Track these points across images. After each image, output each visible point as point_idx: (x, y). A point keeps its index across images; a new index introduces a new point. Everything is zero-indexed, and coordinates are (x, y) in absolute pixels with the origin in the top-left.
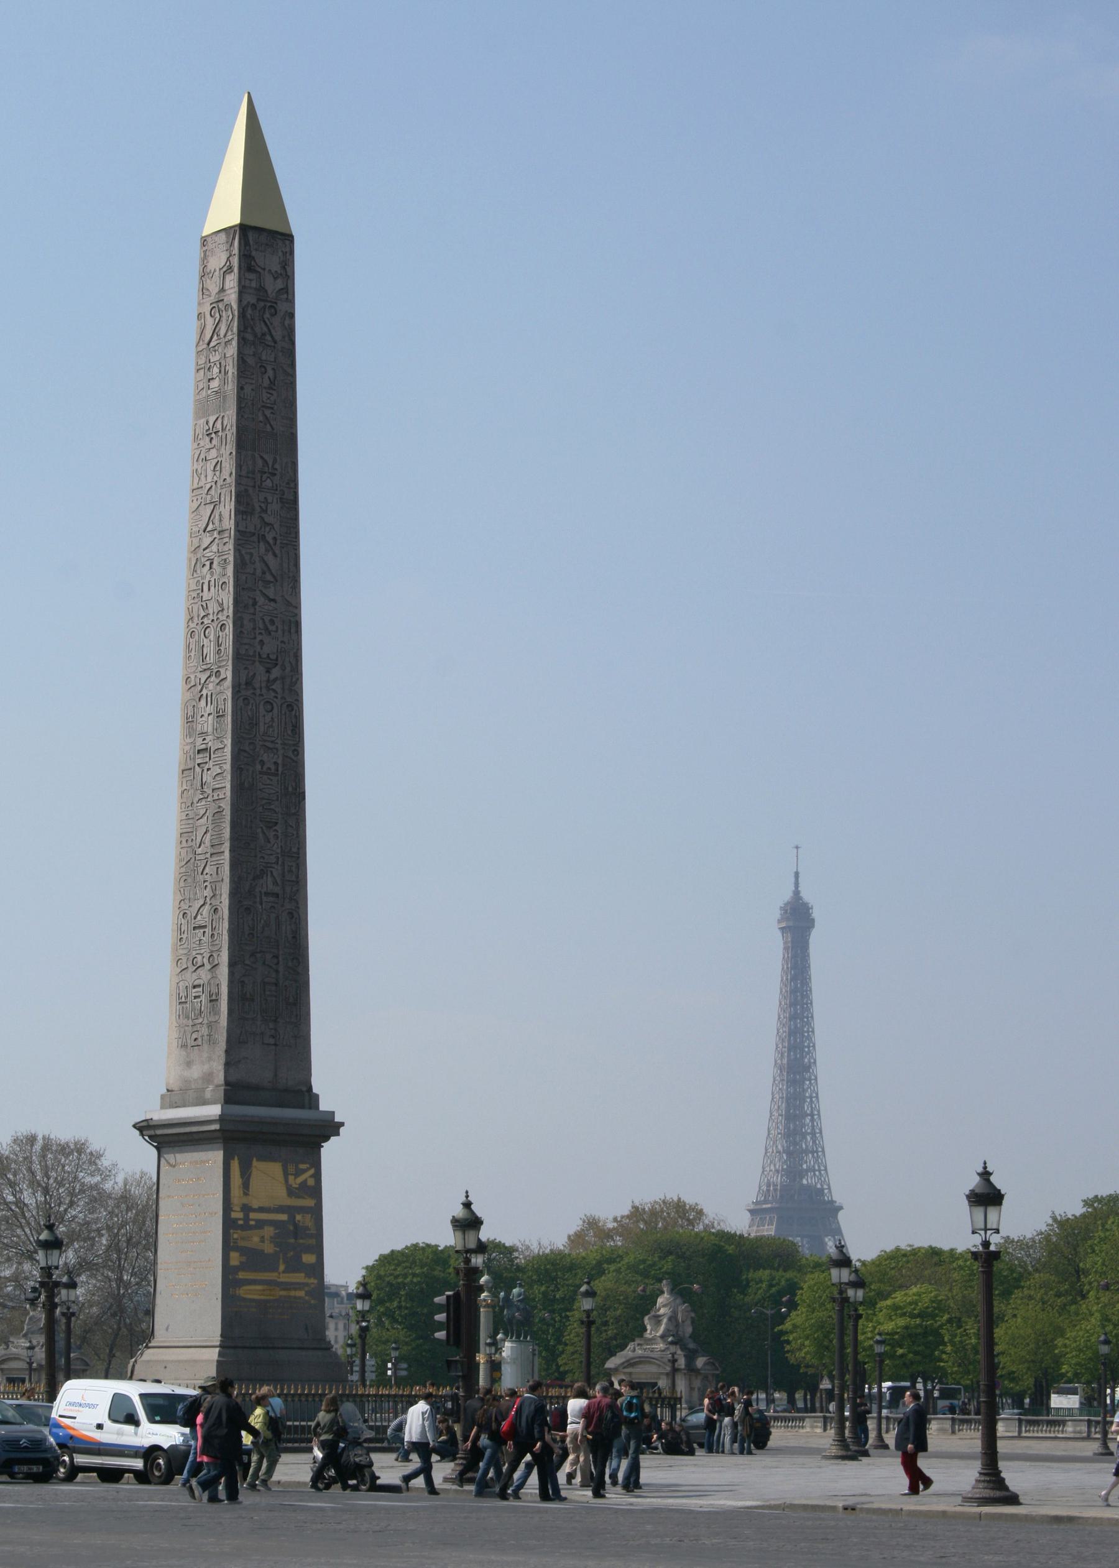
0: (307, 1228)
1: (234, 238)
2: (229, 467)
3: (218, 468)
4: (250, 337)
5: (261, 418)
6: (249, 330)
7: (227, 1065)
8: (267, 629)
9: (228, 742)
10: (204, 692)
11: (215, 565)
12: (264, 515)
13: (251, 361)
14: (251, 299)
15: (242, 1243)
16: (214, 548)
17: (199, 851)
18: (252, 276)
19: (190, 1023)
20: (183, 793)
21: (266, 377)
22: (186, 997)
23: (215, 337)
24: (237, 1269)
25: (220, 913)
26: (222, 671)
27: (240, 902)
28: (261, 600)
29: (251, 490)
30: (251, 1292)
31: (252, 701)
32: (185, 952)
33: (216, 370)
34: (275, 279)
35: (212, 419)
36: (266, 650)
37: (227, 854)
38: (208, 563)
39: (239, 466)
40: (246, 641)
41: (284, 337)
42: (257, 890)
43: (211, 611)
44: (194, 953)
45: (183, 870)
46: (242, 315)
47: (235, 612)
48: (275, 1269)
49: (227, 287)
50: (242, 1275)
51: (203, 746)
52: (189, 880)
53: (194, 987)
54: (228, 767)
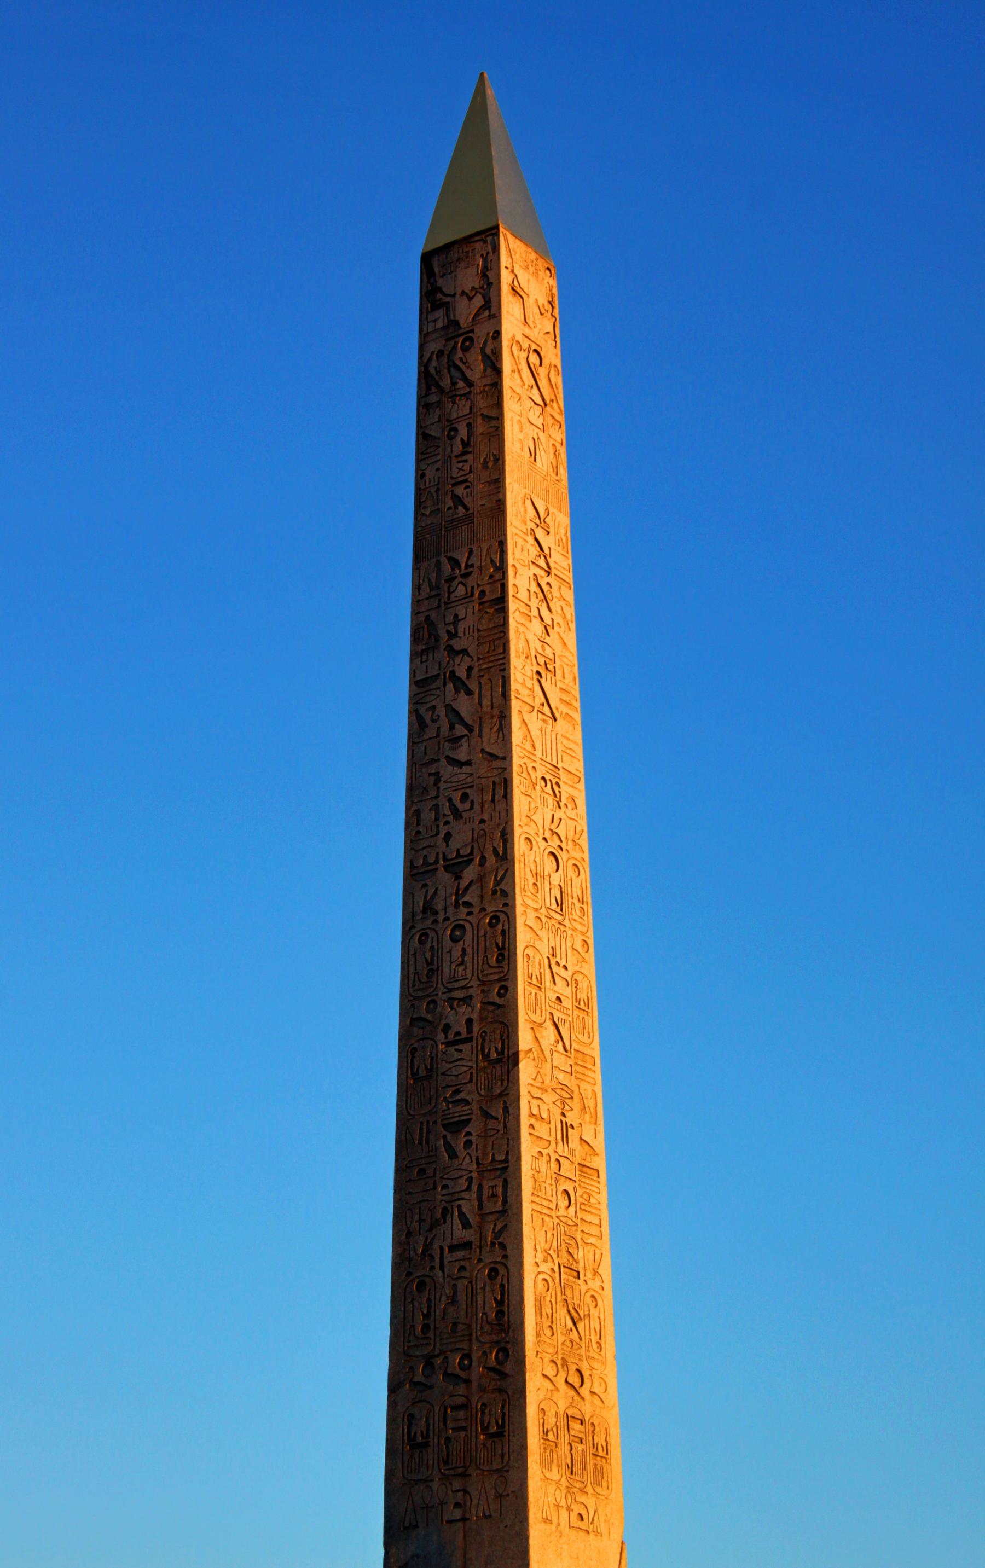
18: (440, 313)
28: (447, 771)
29: (433, 615)
31: (432, 934)
42: (436, 1246)
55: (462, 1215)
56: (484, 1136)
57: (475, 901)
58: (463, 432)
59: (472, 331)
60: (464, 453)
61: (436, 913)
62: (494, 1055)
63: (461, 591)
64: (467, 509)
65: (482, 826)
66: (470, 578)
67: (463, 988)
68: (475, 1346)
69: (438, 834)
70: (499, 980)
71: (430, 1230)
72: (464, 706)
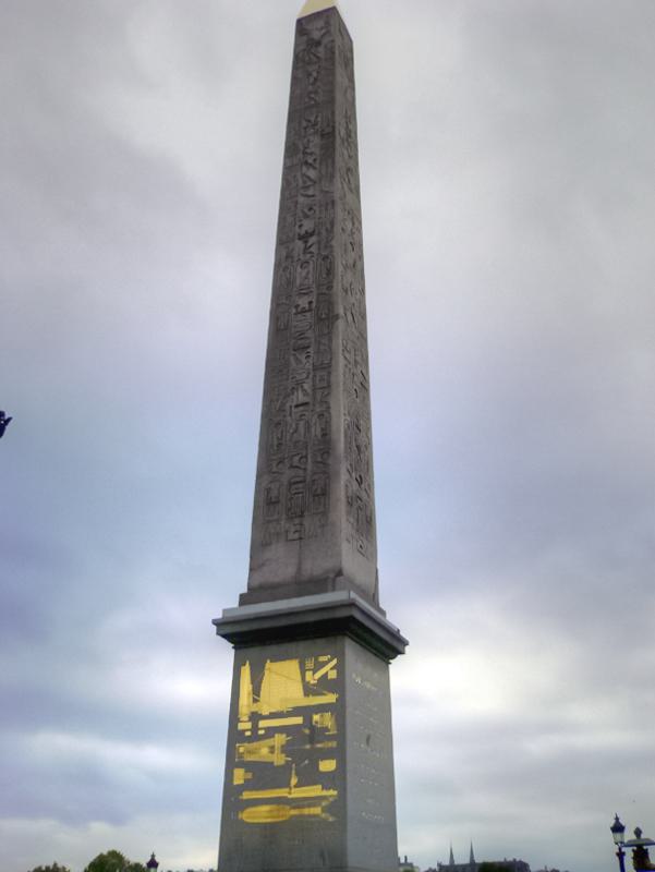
0: (326, 729)
15: (249, 758)
24: (241, 788)
28: (301, 199)
30: (259, 815)
42: (288, 405)
48: (288, 785)
55: (304, 390)
56: (318, 352)
58: (315, 74)
68: (309, 451)
71: (284, 398)
72: (312, 173)
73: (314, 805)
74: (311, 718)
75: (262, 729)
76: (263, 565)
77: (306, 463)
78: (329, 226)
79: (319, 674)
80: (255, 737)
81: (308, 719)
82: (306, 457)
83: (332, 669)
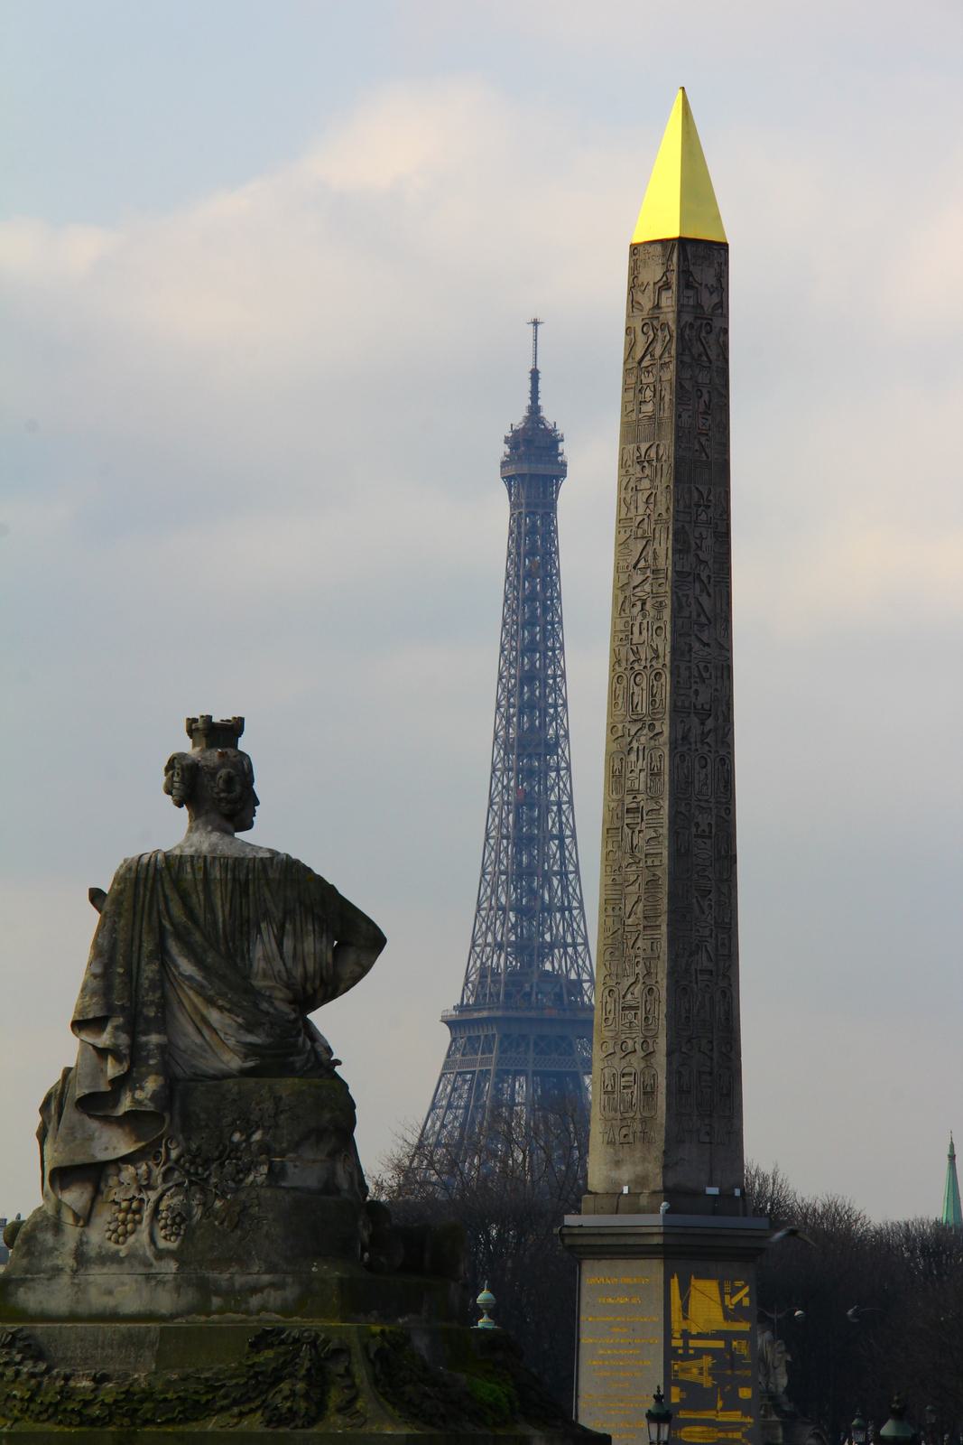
1: (672, 252)
2: (664, 503)
3: (652, 500)
4: (687, 359)
5: (697, 447)
6: (687, 352)
7: (666, 1167)
8: (701, 676)
9: (666, 804)
10: (635, 745)
11: (648, 606)
12: (699, 552)
13: (687, 385)
14: (687, 318)
16: (647, 587)
17: (629, 921)
18: (691, 293)
19: (619, 1117)
20: (608, 854)
21: (702, 401)
22: (613, 1087)
23: (648, 357)
25: (655, 994)
26: (657, 724)
27: (677, 981)
28: (696, 645)
29: (687, 527)
31: (687, 758)
32: (610, 1034)
33: (649, 393)
34: (711, 293)
35: (644, 447)
36: (701, 699)
37: (664, 928)
38: (639, 603)
39: (677, 501)
40: (682, 692)
41: (718, 356)
42: (693, 967)
43: (643, 657)
44: (623, 1037)
45: (609, 941)
46: (681, 337)
47: (672, 661)
49: (664, 303)
50: (683, 1415)
51: (634, 805)
52: (617, 954)
53: (623, 1075)
54: (665, 831)
55: (707, 951)
57: (712, 744)
58: (706, 397)
59: (711, 320)
60: (705, 413)
61: (690, 744)
62: (723, 853)
63: (703, 517)
64: (708, 458)
65: (716, 693)
66: (709, 510)
67: (707, 801)
69: (691, 688)
70: (727, 803)
73: (738, 1430)
74: (731, 1344)
75: (692, 1348)
76: (676, 1164)
77: (712, 1050)
78: (724, 708)
79: (735, 1300)
80: (686, 1357)
81: (729, 1345)
82: (711, 1042)
83: (746, 1296)
